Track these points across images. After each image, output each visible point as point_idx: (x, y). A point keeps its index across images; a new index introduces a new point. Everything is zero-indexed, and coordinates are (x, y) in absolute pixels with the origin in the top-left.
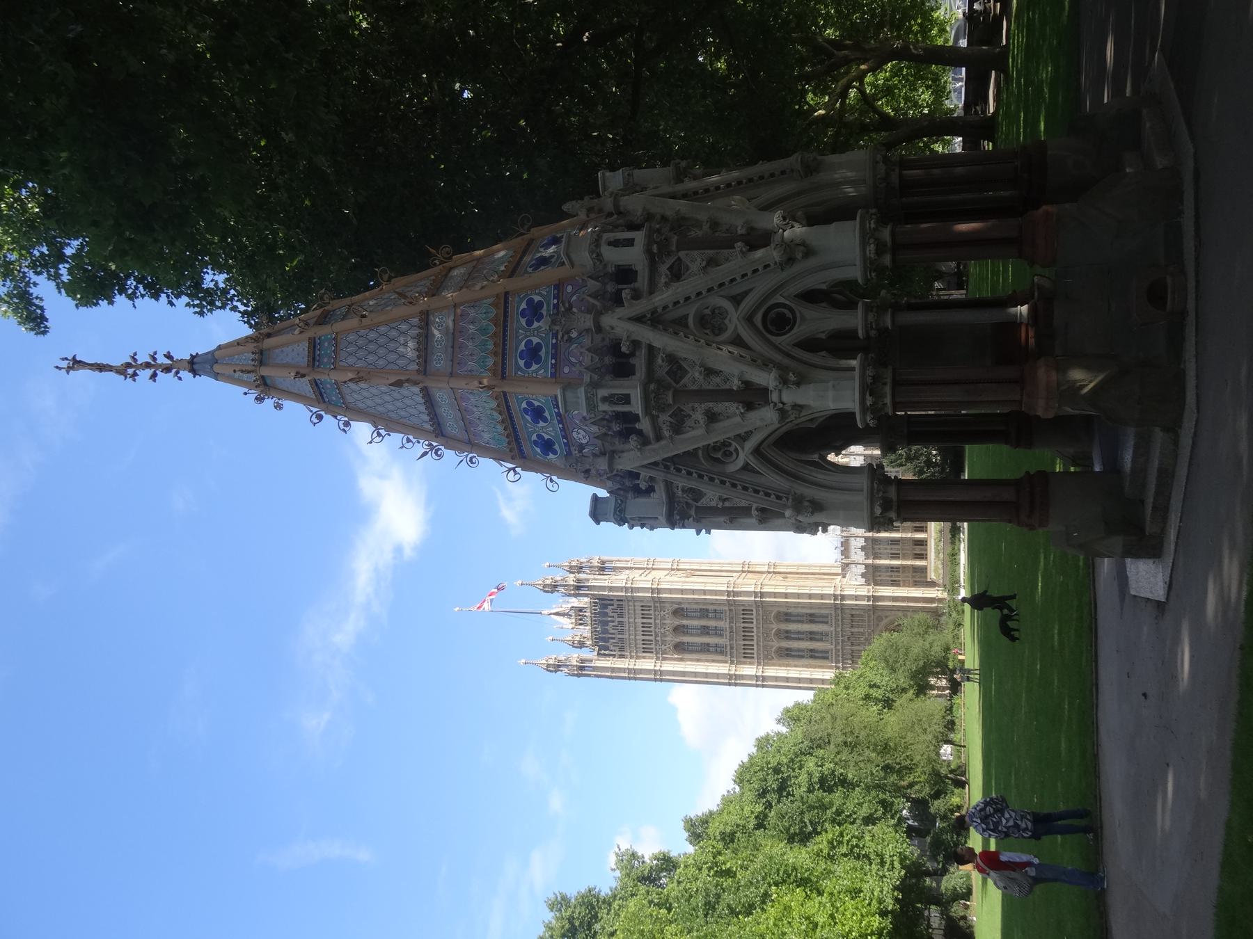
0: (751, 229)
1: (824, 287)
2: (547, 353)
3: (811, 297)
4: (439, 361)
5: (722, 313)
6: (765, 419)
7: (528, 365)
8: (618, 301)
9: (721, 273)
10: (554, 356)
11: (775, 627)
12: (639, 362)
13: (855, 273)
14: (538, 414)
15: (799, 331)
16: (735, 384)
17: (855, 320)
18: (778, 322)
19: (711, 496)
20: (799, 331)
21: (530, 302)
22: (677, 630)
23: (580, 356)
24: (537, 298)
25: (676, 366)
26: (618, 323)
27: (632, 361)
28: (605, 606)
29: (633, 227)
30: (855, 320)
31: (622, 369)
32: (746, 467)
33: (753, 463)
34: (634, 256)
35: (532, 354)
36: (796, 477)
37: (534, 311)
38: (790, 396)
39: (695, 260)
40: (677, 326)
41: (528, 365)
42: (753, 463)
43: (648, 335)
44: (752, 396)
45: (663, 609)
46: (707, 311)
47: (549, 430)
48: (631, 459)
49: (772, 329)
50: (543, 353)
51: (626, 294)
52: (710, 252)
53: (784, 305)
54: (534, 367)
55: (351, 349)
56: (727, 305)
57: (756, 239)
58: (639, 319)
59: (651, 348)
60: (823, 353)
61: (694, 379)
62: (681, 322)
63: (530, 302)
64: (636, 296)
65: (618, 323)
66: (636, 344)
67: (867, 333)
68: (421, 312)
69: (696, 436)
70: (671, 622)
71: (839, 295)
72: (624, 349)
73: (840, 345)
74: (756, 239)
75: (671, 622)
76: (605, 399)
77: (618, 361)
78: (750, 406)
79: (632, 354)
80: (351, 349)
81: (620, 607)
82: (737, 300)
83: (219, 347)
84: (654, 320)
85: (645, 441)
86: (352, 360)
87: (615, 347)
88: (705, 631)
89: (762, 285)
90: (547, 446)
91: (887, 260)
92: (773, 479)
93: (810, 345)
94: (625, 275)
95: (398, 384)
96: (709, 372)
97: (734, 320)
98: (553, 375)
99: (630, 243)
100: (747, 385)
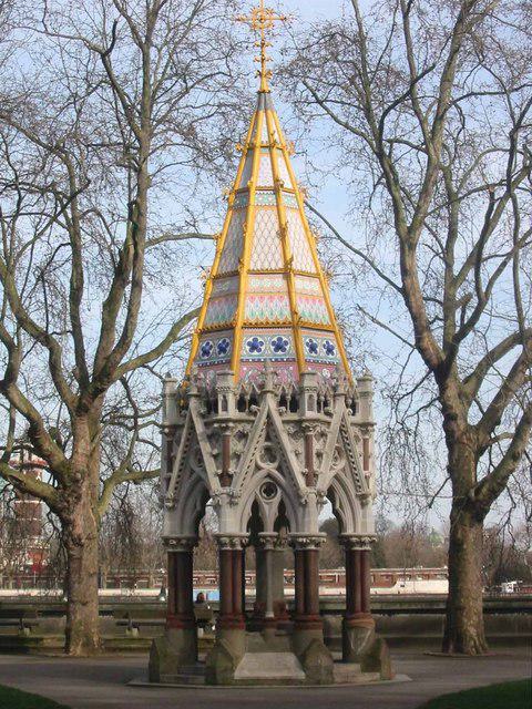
0: (316, 476)
8: (282, 402)
16: (231, 470)
20: (263, 501)
24: (287, 347)
31: (241, 405)
32: (192, 472)
33: (194, 476)
35: (254, 347)
37: (279, 346)
41: (249, 344)
42: (194, 476)
44: (226, 478)
49: (264, 487)
51: (283, 408)
55: (266, 218)
56: (276, 464)
58: (269, 416)
59: (253, 422)
64: (281, 414)
66: (255, 414)
72: (253, 406)
73: (256, 523)
76: (224, 397)
78: (221, 477)
80: (266, 218)
85: (203, 416)
94: (295, 405)
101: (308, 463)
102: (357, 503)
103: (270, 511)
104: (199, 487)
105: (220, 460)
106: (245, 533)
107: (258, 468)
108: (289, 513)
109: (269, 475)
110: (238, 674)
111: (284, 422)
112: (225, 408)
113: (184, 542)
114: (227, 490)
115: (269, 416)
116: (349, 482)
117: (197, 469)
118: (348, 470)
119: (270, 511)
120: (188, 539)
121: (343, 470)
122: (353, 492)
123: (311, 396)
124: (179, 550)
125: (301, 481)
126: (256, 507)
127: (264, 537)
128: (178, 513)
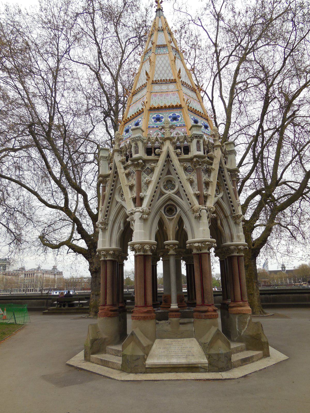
0: (206, 197)
1: (184, 227)
2: (158, 124)
3: (180, 222)
4: (157, 88)
5: (173, 189)
7: (154, 118)
9: (188, 186)
10: (157, 127)
12: (152, 157)
13: (190, 240)
15: (166, 217)
17: (171, 241)
21: (179, 116)
24: (180, 119)
27: (153, 154)
30: (171, 241)
31: (149, 151)
32: (117, 202)
33: (118, 205)
34: (194, 152)
35: (158, 119)
36: (114, 222)
38: (137, 216)
41: (154, 118)
42: (118, 205)
44: (138, 201)
46: (173, 182)
48: (118, 158)
50: (158, 123)
51: (179, 150)
52: (196, 182)
53: (176, 211)
54: (153, 120)
55: (162, 59)
58: (168, 156)
60: (158, 228)
61: (145, 178)
62: (169, 173)
63: (179, 116)
64: (178, 155)
66: (159, 155)
67: (167, 245)
68: (175, 80)
71: (181, 235)
73: (161, 234)
74: (202, 199)
76: (136, 144)
78: (134, 200)
79: (156, 155)
80: (162, 59)
82: (178, 193)
83: (165, 18)
85: (123, 163)
86: (158, 59)
89: (183, 203)
91: (195, 251)
94: (187, 150)
95: (147, 74)
96: (148, 184)
97: (170, 193)
98: (149, 127)
99: (199, 150)
100: (142, 199)
101: (200, 189)
102: (232, 222)
103: (171, 228)
104: (121, 214)
105: (135, 189)
106: (153, 241)
107: (162, 194)
108: (187, 226)
109: (170, 199)
110: (150, 361)
111: (180, 160)
112: (137, 152)
113: (111, 252)
114: (140, 209)
115: (168, 156)
116: (225, 206)
117: (119, 200)
118: (225, 198)
119: (171, 228)
120: (114, 250)
121: (222, 198)
122: (228, 213)
123: (198, 142)
124: (108, 258)
125: (196, 202)
126: (161, 224)
127: (168, 245)
128: (108, 233)
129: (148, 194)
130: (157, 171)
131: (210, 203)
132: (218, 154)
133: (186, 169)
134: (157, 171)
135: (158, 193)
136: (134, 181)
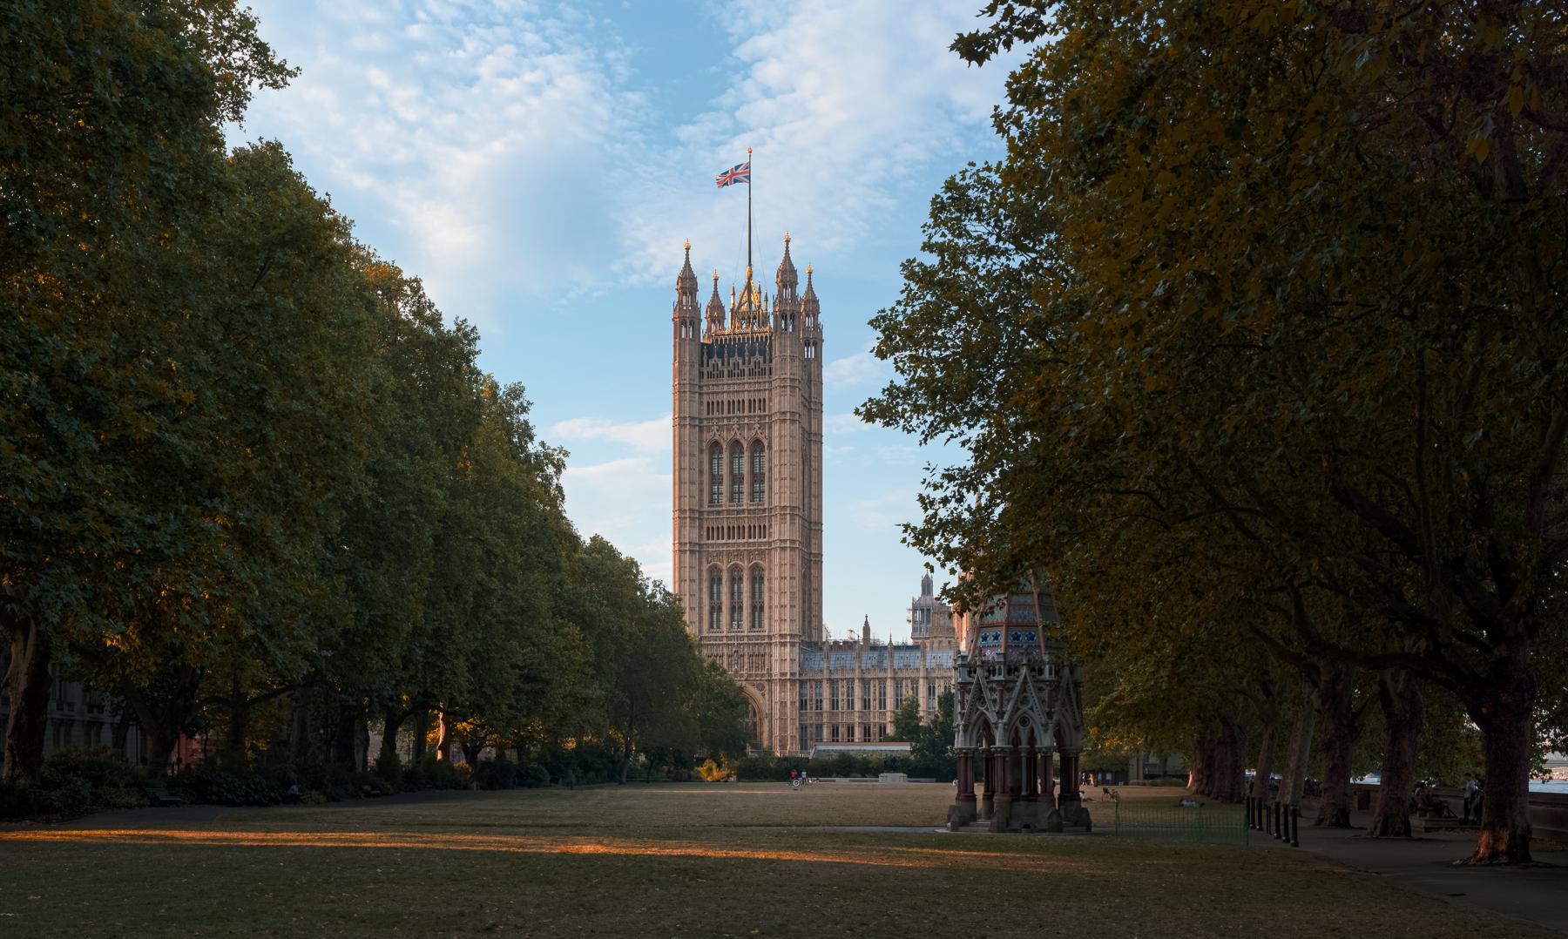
3: (1032, 731)
6: (993, 718)
8: (1033, 670)
11: (745, 564)
12: (1012, 677)
14: (996, 638)
17: (1024, 745)
18: (1024, 721)
19: (968, 697)
22: (736, 445)
23: (1014, 656)
25: (1010, 690)
26: (1024, 671)
28: (762, 353)
29: (1057, 672)
30: (1024, 745)
31: (1009, 671)
34: (1046, 675)
39: (1045, 695)
40: (1024, 689)
43: (1021, 679)
44: (1000, 714)
45: (762, 427)
47: (991, 639)
57: (1049, 715)
65: (1024, 671)
69: (988, 695)
70: (745, 437)
71: (1032, 740)
73: (1016, 741)
75: (745, 437)
77: (1012, 670)
81: (762, 373)
84: (1025, 682)
87: (1017, 670)
88: (736, 479)
90: (985, 639)
92: (974, 717)
93: (1017, 731)
94: (1041, 672)
97: (1025, 708)
129: (1009, 707)
130: (1017, 690)
131: (1055, 717)
132: (1066, 671)
133: (1040, 689)
134: (1017, 690)
135: (1016, 709)
136: (996, 696)
